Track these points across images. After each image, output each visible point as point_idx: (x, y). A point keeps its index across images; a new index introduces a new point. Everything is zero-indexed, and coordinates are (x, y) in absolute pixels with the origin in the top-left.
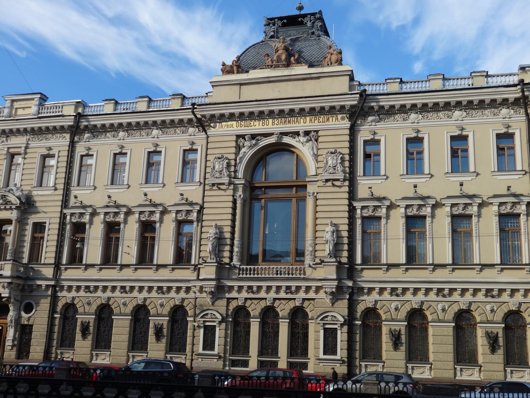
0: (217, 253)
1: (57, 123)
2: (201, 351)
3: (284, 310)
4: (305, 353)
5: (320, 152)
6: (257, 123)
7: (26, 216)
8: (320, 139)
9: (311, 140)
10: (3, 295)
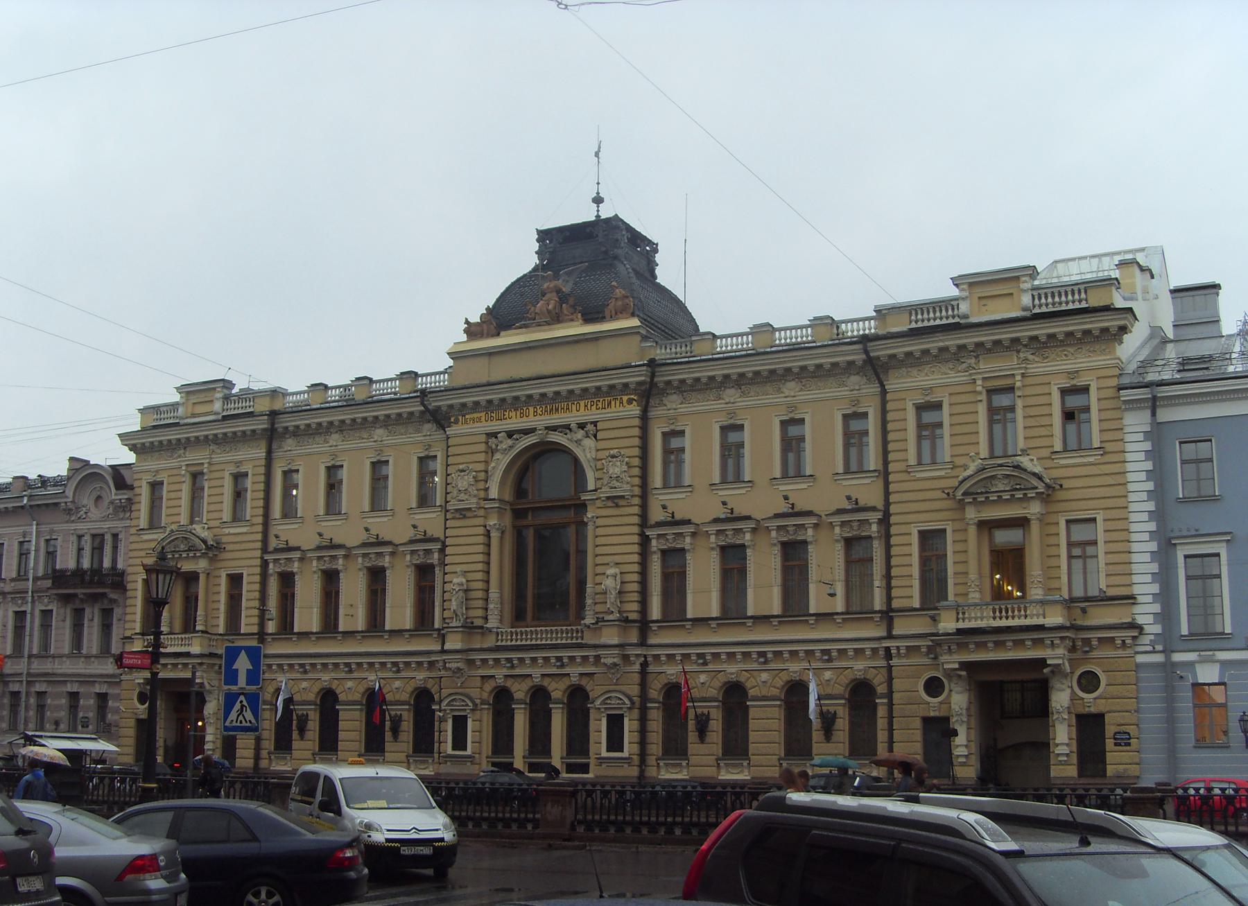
2: (450, 751)
3: (557, 690)
4: (585, 752)
6: (513, 414)
7: (219, 565)
9: (588, 437)
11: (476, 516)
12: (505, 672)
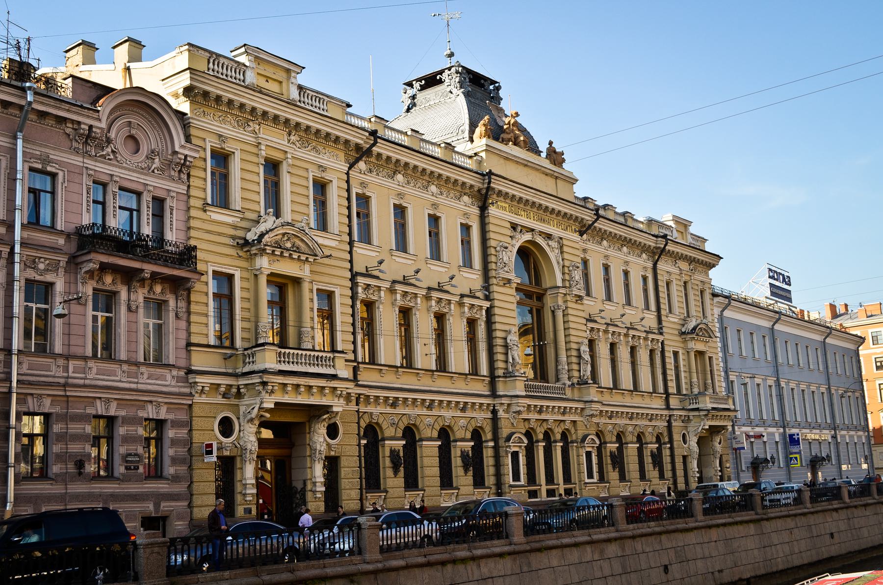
1: (344, 134)
5: (567, 263)
6: (523, 213)
10: (335, 409)
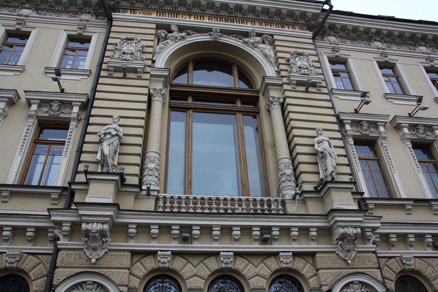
0: (116, 164)
8: (277, 43)
9: (264, 43)
11: (139, 78)
12: (176, 246)
